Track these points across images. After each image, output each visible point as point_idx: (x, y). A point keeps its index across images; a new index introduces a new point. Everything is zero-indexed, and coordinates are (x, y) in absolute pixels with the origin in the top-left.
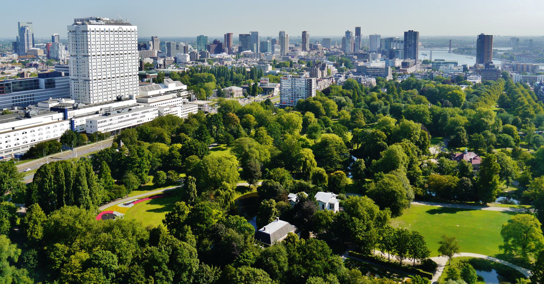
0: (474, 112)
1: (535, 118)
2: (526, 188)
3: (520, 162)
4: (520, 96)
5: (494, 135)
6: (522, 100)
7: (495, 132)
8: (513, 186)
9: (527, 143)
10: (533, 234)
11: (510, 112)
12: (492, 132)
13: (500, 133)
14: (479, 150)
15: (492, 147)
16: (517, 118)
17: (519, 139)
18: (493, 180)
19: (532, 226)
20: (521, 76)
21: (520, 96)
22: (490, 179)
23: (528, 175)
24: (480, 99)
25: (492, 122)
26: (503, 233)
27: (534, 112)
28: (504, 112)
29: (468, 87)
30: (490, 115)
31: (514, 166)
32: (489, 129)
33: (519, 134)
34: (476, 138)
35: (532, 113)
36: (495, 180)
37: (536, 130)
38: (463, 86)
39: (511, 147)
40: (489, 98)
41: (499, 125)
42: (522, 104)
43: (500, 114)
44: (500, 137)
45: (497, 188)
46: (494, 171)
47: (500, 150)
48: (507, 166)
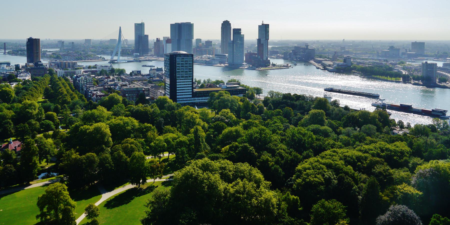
0: (21, 105)
1: (71, 103)
2: (61, 161)
3: (57, 141)
4: (60, 88)
5: (38, 123)
6: (61, 91)
7: (39, 120)
8: (51, 162)
9: (65, 125)
10: (62, 197)
11: (51, 102)
12: (36, 120)
13: (44, 120)
14: (25, 137)
15: (36, 132)
16: (57, 106)
17: (59, 122)
18: (33, 161)
19: (60, 191)
20: (64, 71)
21: (60, 88)
22: (31, 160)
23: (63, 151)
24: (27, 93)
25: (35, 112)
26: (38, 204)
27: (70, 99)
28: (48, 102)
29: (18, 84)
30: (34, 106)
31: (51, 145)
32: (34, 119)
33: (59, 119)
34: (22, 127)
35: (68, 100)
36: (35, 161)
37: (71, 114)
38: (14, 83)
39: (52, 130)
40: (35, 92)
41: (42, 113)
42: (62, 93)
43: (43, 104)
44: (43, 124)
45: (37, 167)
46: (33, 154)
47: (42, 135)
48: (45, 147)
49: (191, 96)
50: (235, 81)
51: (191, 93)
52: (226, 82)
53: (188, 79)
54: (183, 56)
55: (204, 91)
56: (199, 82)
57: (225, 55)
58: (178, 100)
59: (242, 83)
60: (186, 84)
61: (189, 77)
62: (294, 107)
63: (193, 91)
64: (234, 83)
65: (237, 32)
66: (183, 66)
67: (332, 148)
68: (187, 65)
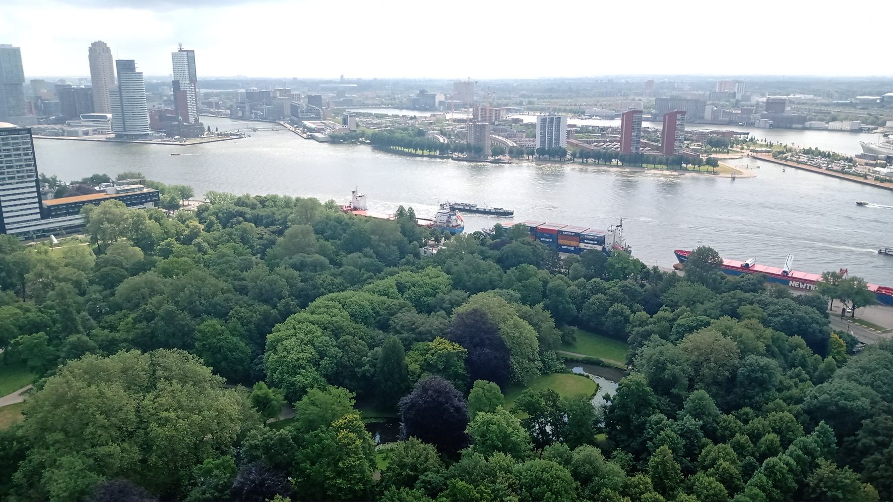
49: (39, 216)
50: (132, 176)
51: (38, 210)
52: (113, 178)
53: (26, 182)
54: (7, 133)
55: (67, 205)
56: (53, 182)
57: (105, 117)
58: (7, 228)
59: (148, 179)
60: (23, 193)
61: (29, 176)
62: (257, 221)
63: (41, 207)
64: (131, 180)
65: (127, 66)
66: (10, 156)
67: (330, 291)
68: (18, 152)
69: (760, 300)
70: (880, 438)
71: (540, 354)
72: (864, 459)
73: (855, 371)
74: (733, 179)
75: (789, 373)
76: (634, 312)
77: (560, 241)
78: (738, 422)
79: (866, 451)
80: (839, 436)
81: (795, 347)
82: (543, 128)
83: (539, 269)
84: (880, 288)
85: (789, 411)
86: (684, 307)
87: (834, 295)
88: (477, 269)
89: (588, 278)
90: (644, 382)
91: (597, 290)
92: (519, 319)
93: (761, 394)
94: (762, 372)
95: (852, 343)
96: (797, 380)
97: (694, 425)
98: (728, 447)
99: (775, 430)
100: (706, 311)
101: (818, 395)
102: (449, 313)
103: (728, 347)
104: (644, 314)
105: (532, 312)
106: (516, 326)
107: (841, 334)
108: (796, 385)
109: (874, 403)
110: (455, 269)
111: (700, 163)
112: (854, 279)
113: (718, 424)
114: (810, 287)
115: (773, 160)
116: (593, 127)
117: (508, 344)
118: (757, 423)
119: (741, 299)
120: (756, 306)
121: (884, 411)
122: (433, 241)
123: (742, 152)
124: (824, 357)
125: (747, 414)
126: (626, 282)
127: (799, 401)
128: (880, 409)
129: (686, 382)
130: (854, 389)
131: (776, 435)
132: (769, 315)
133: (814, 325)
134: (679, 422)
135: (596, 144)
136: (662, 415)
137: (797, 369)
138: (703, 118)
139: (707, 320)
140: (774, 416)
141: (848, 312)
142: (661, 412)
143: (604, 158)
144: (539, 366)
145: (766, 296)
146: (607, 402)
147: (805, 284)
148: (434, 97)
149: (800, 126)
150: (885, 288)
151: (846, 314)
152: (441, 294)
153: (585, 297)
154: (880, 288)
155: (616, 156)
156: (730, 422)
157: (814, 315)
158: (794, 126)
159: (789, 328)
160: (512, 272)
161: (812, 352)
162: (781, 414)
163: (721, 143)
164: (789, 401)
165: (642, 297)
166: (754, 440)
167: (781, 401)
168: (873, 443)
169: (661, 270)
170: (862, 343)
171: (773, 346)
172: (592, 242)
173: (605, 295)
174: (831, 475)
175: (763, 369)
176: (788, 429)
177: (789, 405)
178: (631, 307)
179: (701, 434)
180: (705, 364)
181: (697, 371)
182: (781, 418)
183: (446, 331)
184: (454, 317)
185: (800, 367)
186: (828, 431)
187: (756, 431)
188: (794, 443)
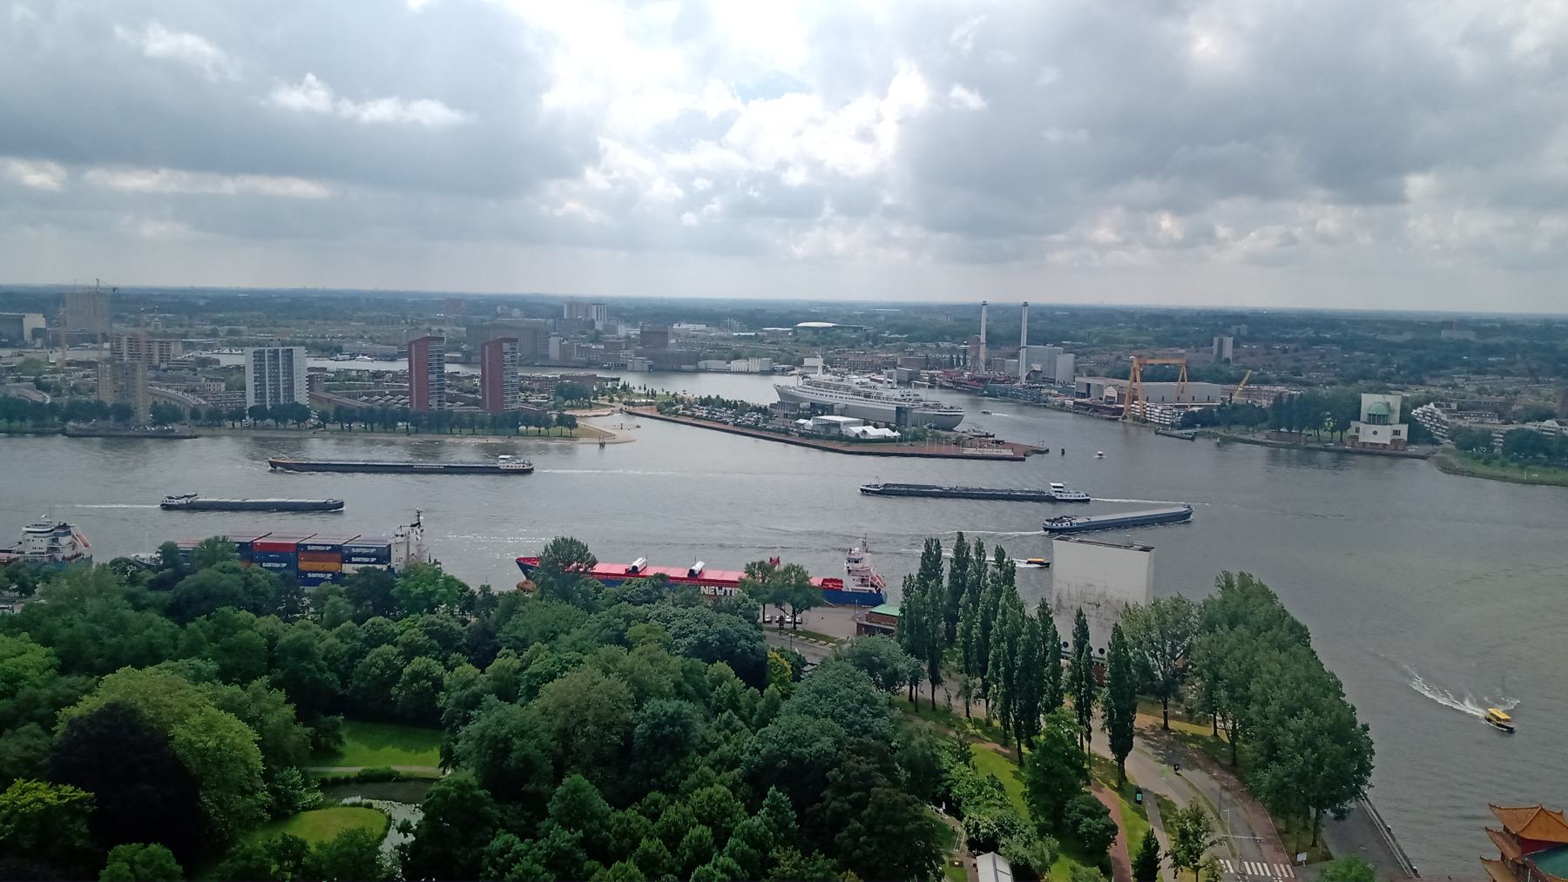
69: (659, 615)
70: (855, 795)
71: (267, 776)
72: (837, 835)
73: (807, 698)
74: (602, 445)
75: (715, 723)
76: (450, 669)
77: (303, 566)
78: (643, 819)
79: (839, 822)
80: (798, 806)
81: (719, 681)
82: (259, 368)
83: (258, 617)
84: (825, 580)
85: (722, 783)
86: (538, 644)
87: (765, 596)
88: (120, 627)
89: (360, 620)
90: (473, 781)
91: (375, 640)
92: (214, 711)
93: (675, 765)
94: (673, 726)
95: (799, 664)
96: (728, 732)
97: (568, 841)
98: (631, 866)
99: (702, 821)
100: (574, 644)
101: (760, 746)
102: (48, 723)
103: (613, 692)
104: (468, 670)
105: (247, 696)
106: (209, 728)
107: (781, 651)
108: (727, 739)
109: (839, 743)
110: (65, 633)
111: (547, 423)
112: (790, 569)
113: (609, 829)
114: (731, 591)
115: (658, 415)
116: (358, 371)
117: (193, 764)
118: (673, 813)
119: (629, 615)
120: (653, 622)
121: (853, 751)
122: (15, 590)
123: (611, 406)
124: (762, 687)
125: (655, 803)
126: (433, 618)
127: (734, 763)
128: (848, 749)
129: (548, 766)
130: (811, 727)
131: (705, 828)
132: (676, 636)
133: (743, 642)
134: (541, 843)
135: (365, 398)
136: (511, 837)
137: (727, 714)
138: (546, 357)
139: (577, 658)
140: (698, 796)
141: (788, 622)
142: (509, 832)
143: (381, 420)
144: (266, 802)
145: (667, 608)
146: (406, 836)
147: (724, 588)
148: (20, 321)
149: (692, 367)
150: (831, 580)
151: (785, 626)
152: (29, 689)
153: (357, 655)
154: (825, 580)
155: (404, 415)
156: (629, 822)
157: (740, 627)
158: (684, 367)
159: (704, 651)
160: (199, 626)
161: (744, 684)
162: (709, 790)
163: (578, 394)
164: (719, 766)
165: (464, 640)
166: (671, 845)
167: (707, 768)
168: (847, 806)
169: (495, 590)
170: (812, 664)
171: (686, 684)
172: (367, 560)
173: (395, 645)
174: (796, 871)
175: (674, 719)
176: (724, 813)
177: (719, 773)
178: (444, 661)
179: (581, 855)
180: (578, 729)
181: (566, 747)
182: (710, 797)
183: (39, 763)
184: (61, 728)
185: (730, 711)
186: (782, 802)
187: (673, 828)
188: (734, 834)
